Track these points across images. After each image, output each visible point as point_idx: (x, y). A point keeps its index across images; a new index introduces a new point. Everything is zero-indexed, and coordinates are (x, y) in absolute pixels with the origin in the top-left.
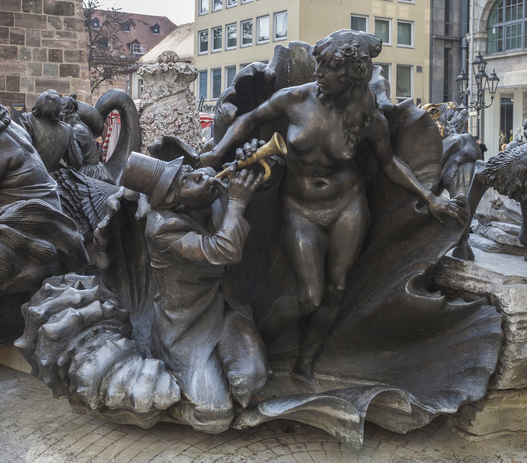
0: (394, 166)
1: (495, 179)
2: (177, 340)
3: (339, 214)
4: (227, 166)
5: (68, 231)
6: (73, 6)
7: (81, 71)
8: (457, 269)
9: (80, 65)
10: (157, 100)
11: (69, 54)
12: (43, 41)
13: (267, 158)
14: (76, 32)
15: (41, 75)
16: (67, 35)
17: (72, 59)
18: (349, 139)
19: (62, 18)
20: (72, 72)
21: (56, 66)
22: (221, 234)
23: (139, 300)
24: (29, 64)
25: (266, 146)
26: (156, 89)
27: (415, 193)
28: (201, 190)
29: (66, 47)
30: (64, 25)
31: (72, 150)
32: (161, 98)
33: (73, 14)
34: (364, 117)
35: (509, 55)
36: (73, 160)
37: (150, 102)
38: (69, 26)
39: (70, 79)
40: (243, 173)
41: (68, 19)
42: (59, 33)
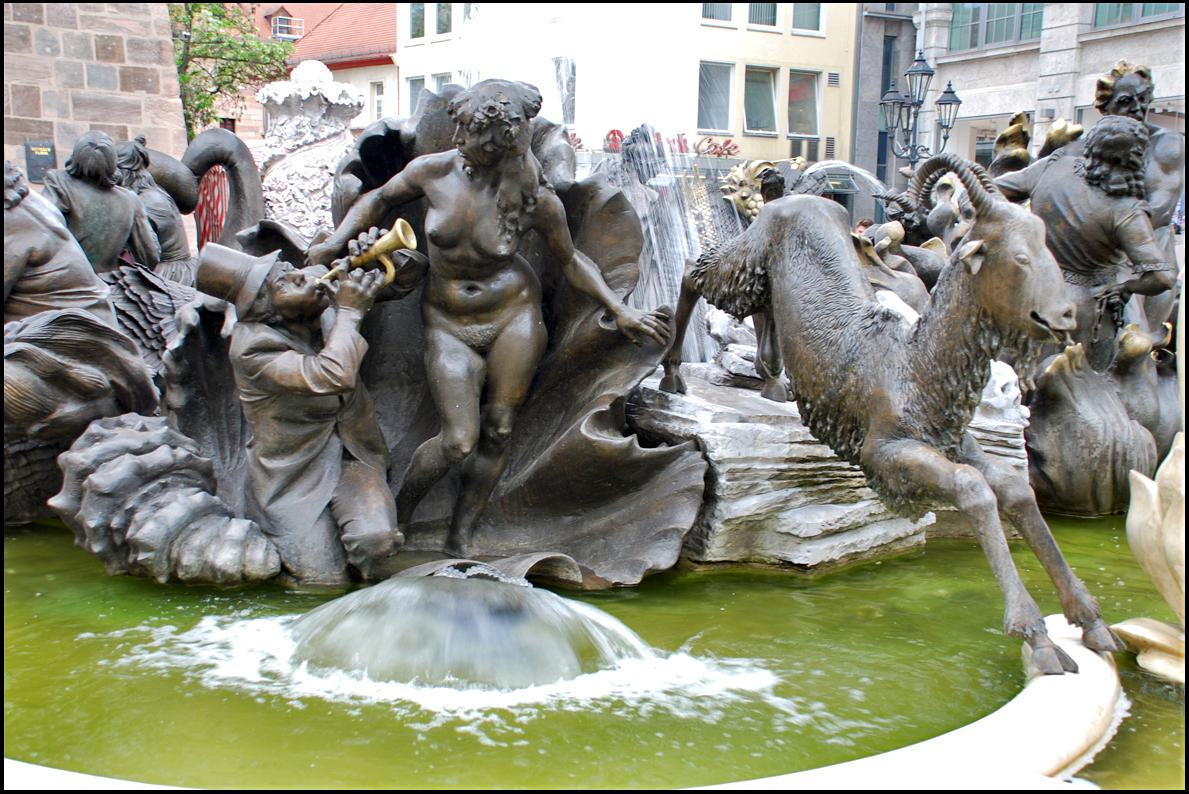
0: (575, 264)
1: (703, 283)
2: (278, 495)
3: (501, 330)
4: (337, 264)
5: (124, 354)
7: (162, 81)
8: (668, 408)
9: (159, 68)
10: (293, 151)
11: (136, 45)
13: (389, 253)
15: (81, 85)
17: (143, 56)
18: (505, 229)
20: (145, 82)
21: (113, 69)
22: (325, 352)
23: (232, 453)
24: (58, 64)
25: (387, 237)
26: (290, 129)
27: (601, 303)
28: (303, 296)
29: (129, 31)
31: (140, 236)
32: (299, 146)
34: (525, 200)
35: (989, 54)
36: (144, 253)
37: (277, 152)
39: (139, 96)
40: (358, 272)
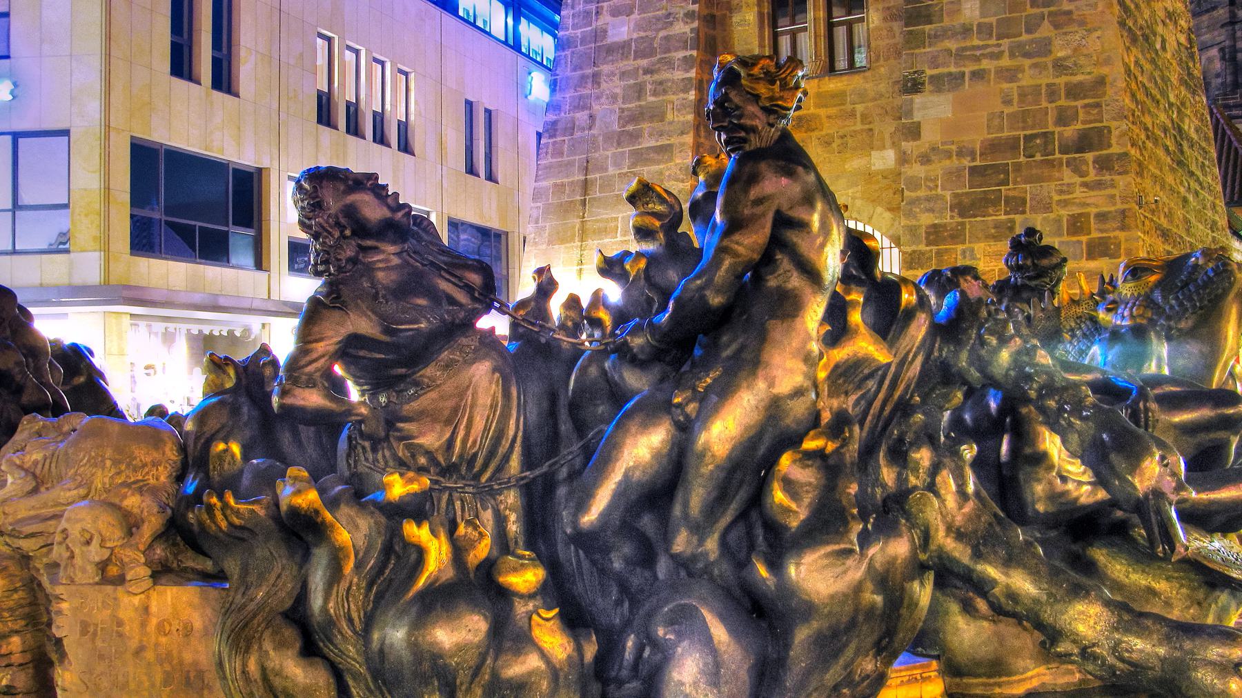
6: (1110, 132)
11: (1102, 217)
12: (1059, 202)
14: (1114, 177)
16: (1099, 185)
17: (1108, 226)
19: (1090, 156)
20: (1108, 248)
21: (1080, 242)
30: (1094, 167)
33: (1110, 146)
38: (1101, 169)
41: (1100, 156)
42: (1085, 185)
